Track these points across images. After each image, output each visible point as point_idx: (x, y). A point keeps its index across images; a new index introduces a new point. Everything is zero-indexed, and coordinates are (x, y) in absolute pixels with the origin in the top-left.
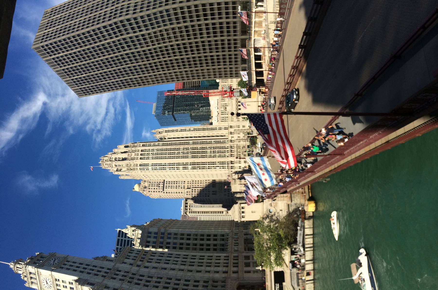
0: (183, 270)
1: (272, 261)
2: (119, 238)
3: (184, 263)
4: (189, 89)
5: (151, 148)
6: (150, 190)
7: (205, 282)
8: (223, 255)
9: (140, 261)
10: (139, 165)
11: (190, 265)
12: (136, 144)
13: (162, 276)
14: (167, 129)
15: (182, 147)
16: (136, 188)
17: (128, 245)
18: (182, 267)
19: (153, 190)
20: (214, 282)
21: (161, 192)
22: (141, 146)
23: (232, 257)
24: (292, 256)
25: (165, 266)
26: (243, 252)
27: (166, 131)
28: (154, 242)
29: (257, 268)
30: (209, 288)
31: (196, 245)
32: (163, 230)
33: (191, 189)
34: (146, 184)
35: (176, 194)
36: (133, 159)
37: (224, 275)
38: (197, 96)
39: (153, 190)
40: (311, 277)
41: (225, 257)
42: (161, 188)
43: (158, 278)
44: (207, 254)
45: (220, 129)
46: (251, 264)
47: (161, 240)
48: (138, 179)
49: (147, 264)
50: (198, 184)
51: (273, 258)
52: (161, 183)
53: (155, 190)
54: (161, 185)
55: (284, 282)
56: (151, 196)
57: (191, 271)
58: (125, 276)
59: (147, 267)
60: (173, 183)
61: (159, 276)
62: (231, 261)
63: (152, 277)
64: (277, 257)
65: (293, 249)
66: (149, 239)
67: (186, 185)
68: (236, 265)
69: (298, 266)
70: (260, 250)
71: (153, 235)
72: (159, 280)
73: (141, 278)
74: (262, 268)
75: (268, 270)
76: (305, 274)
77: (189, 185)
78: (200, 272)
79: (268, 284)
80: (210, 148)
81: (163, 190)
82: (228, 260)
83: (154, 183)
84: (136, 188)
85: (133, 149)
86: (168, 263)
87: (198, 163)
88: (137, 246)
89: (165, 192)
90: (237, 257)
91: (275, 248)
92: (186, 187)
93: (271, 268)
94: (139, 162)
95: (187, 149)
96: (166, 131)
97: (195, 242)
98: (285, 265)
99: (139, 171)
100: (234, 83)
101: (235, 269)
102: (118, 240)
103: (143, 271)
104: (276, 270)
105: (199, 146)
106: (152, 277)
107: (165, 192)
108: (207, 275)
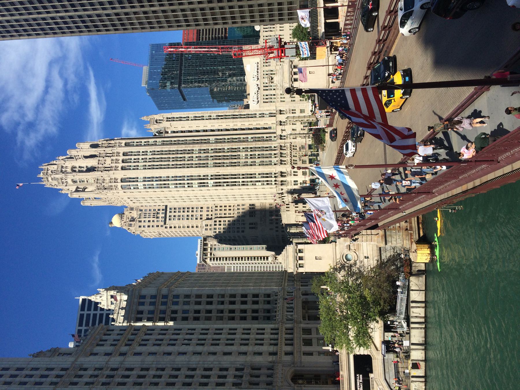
0: (200, 353)
1: (351, 339)
2: (82, 312)
3: (203, 342)
4: (208, 44)
5: (141, 149)
6: (142, 224)
7: (237, 370)
8: (268, 326)
9: (126, 345)
10: (119, 181)
11: (212, 345)
12: (112, 142)
13: (164, 366)
14: (169, 115)
15: (197, 147)
16: (116, 221)
17: (101, 321)
18: (199, 349)
19: (147, 224)
20: (253, 369)
21: (162, 226)
22: (123, 145)
23: (284, 329)
24: (386, 334)
25: (170, 349)
26: (301, 323)
27: (168, 119)
28: (150, 312)
29: (324, 348)
30: (244, 378)
31: (222, 311)
32: (165, 291)
33: (213, 220)
34: (135, 214)
35: (187, 229)
36: (108, 169)
37: (271, 358)
38: (223, 55)
39: (147, 224)
40: (420, 372)
41: (272, 329)
42: (160, 219)
43: (158, 369)
44: (240, 326)
45: (262, 115)
46: (314, 341)
47: (163, 308)
48: (119, 205)
49: (139, 349)
50: (225, 212)
51: (352, 334)
52: (161, 212)
53: (151, 224)
54: (161, 215)
55: (372, 372)
56: (142, 235)
57: (214, 354)
58: (96, 376)
59: (140, 354)
60: (182, 210)
61: (160, 366)
62: (283, 336)
63: (147, 369)
64: (359, 333)
65: (389, 323)
66: (141, 308)
67: (204, 214)
68: (290, 342)
69: (397, 350)
70: (331, 318)
71: (148, 300)
72: (159, 373)
73: (127, 373)
74: (333, 347)
75: (343, 353)
76: (410, 366)
78: (230, 354)
79: (343, 373)
80: (246, 149)
81: (165, 223)
82: (277, 334)
83: (148, 212)
84: (116, 221)
85: (109, 150)
86: (174, 345)
87: (225, 177)
88: (120, 321)
89: (168, 226)
90: (292, 329)
91: (356, 319)
92: (205, 217)
93: (350, 349)
94: (120, 174)
95: (206, 151)
96: (168, 119)
97: (221, 307)
98: (372, 346)
99: (121, 191)
100: (285, 31)
101: (289, 349)
102: (82, 316)
104: (358, 353)
105: (226, 146)
106: (147, 369)
107: (168, 226)
108: (241, 359)
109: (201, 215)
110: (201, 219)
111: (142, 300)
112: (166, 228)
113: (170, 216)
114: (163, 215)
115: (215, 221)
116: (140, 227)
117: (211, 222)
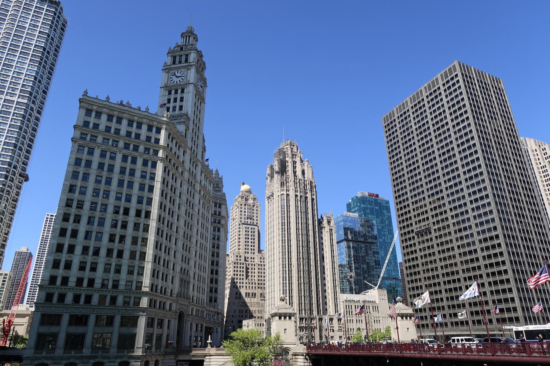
6: (243, 206)
19: (243, 210)
21: (241, 221)
34: (251, 202)
42: (246, 220)
49: (201, 202)
52: (252, 221)
53: (243, 213)
67: (249, 255)
74: (210, 343)
77: (249, 260)
81: (243, 224)
89: (241, 226)
92: (247, 255)
96: (331, 230)
103: (197, 196)
109: (248, 253)
110: (245, 252)
111: (218, 205)
112: (240, 225)
113: (248, 228)
114: (249, 223)
115: (243, 264)
116: (241, 205)
117: (243, 261)
